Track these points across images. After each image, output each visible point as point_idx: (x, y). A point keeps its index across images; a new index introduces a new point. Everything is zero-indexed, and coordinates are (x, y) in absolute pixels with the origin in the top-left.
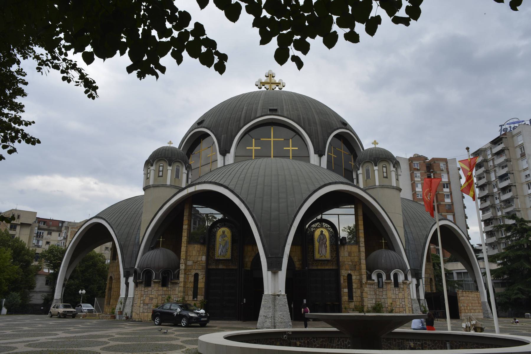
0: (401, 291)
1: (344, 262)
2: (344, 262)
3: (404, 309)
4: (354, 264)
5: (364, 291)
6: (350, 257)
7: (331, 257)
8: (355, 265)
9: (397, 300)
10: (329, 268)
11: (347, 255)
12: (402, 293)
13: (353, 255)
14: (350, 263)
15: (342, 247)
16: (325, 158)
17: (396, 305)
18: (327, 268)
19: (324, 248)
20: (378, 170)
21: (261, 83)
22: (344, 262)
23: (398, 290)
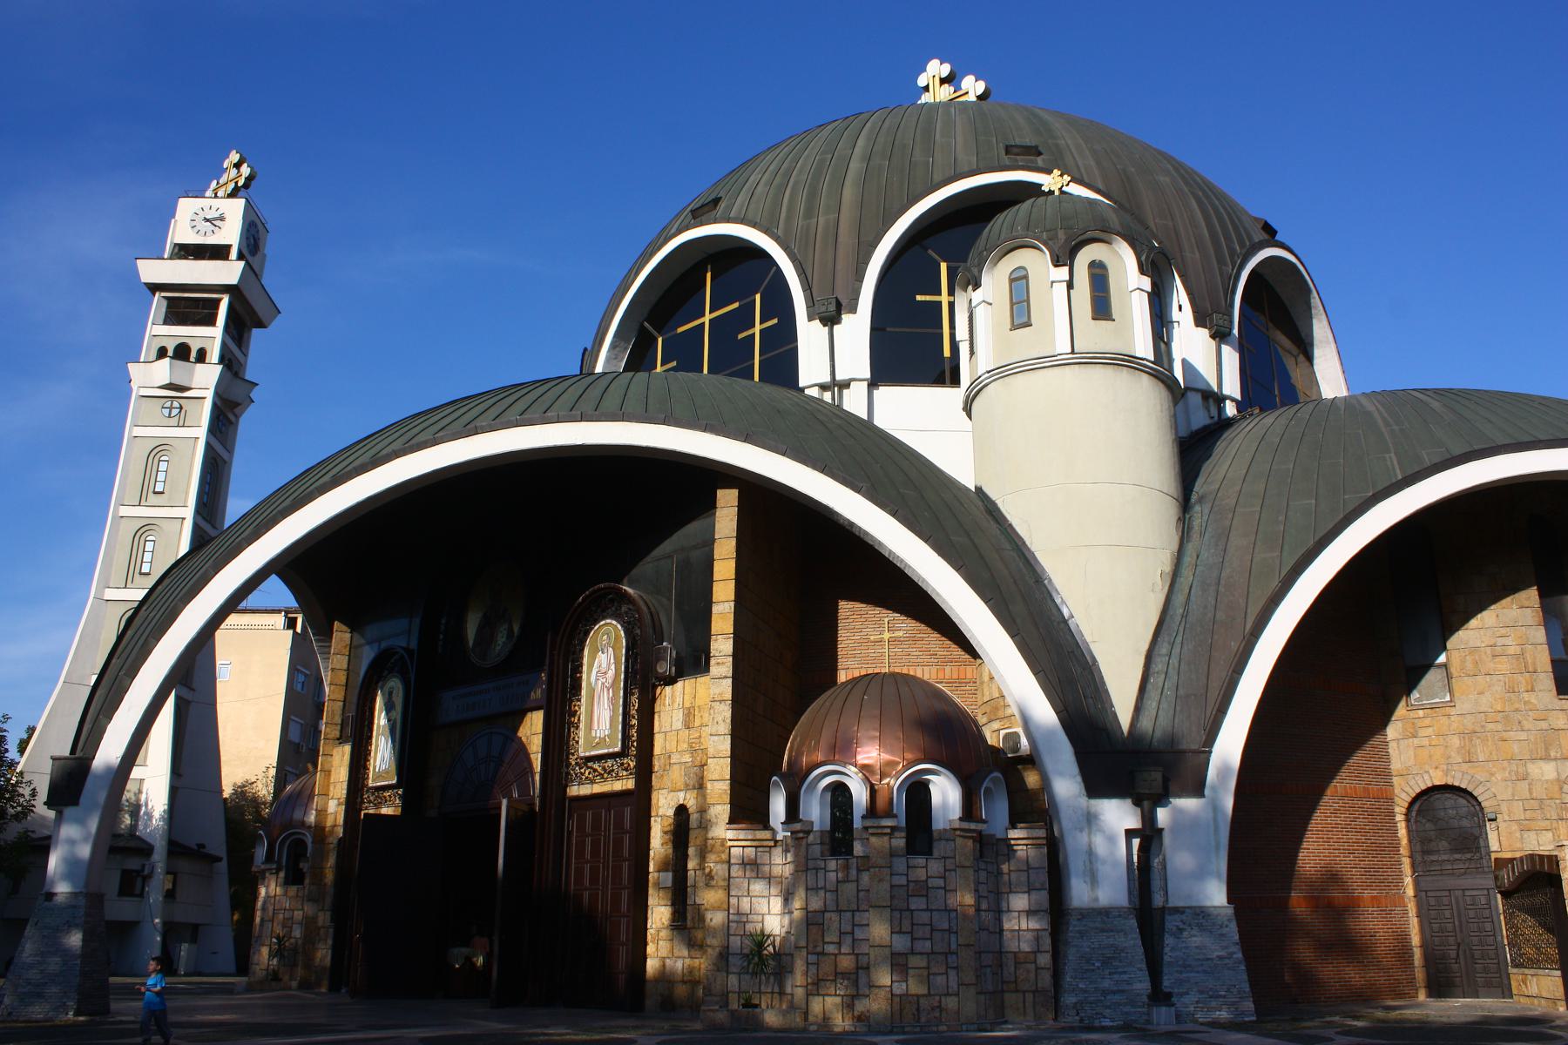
0: (853, 872)
1: (670, 756)
3: (864, 960)
4: (698, 763)
5: (713, 879)
6: (687, 731)
7: (626, 737)
8: (703, 766)
9: (831, 919)
10: (624, 788)
11: (678, 724)
12: (857, 881)
13: (696, 725)
14: (687, 758)
15: (668, 689)
16: (856, 329)
17: (824, 943)
18: (618, 786)
19: (606, 705)
23: (836, 871)
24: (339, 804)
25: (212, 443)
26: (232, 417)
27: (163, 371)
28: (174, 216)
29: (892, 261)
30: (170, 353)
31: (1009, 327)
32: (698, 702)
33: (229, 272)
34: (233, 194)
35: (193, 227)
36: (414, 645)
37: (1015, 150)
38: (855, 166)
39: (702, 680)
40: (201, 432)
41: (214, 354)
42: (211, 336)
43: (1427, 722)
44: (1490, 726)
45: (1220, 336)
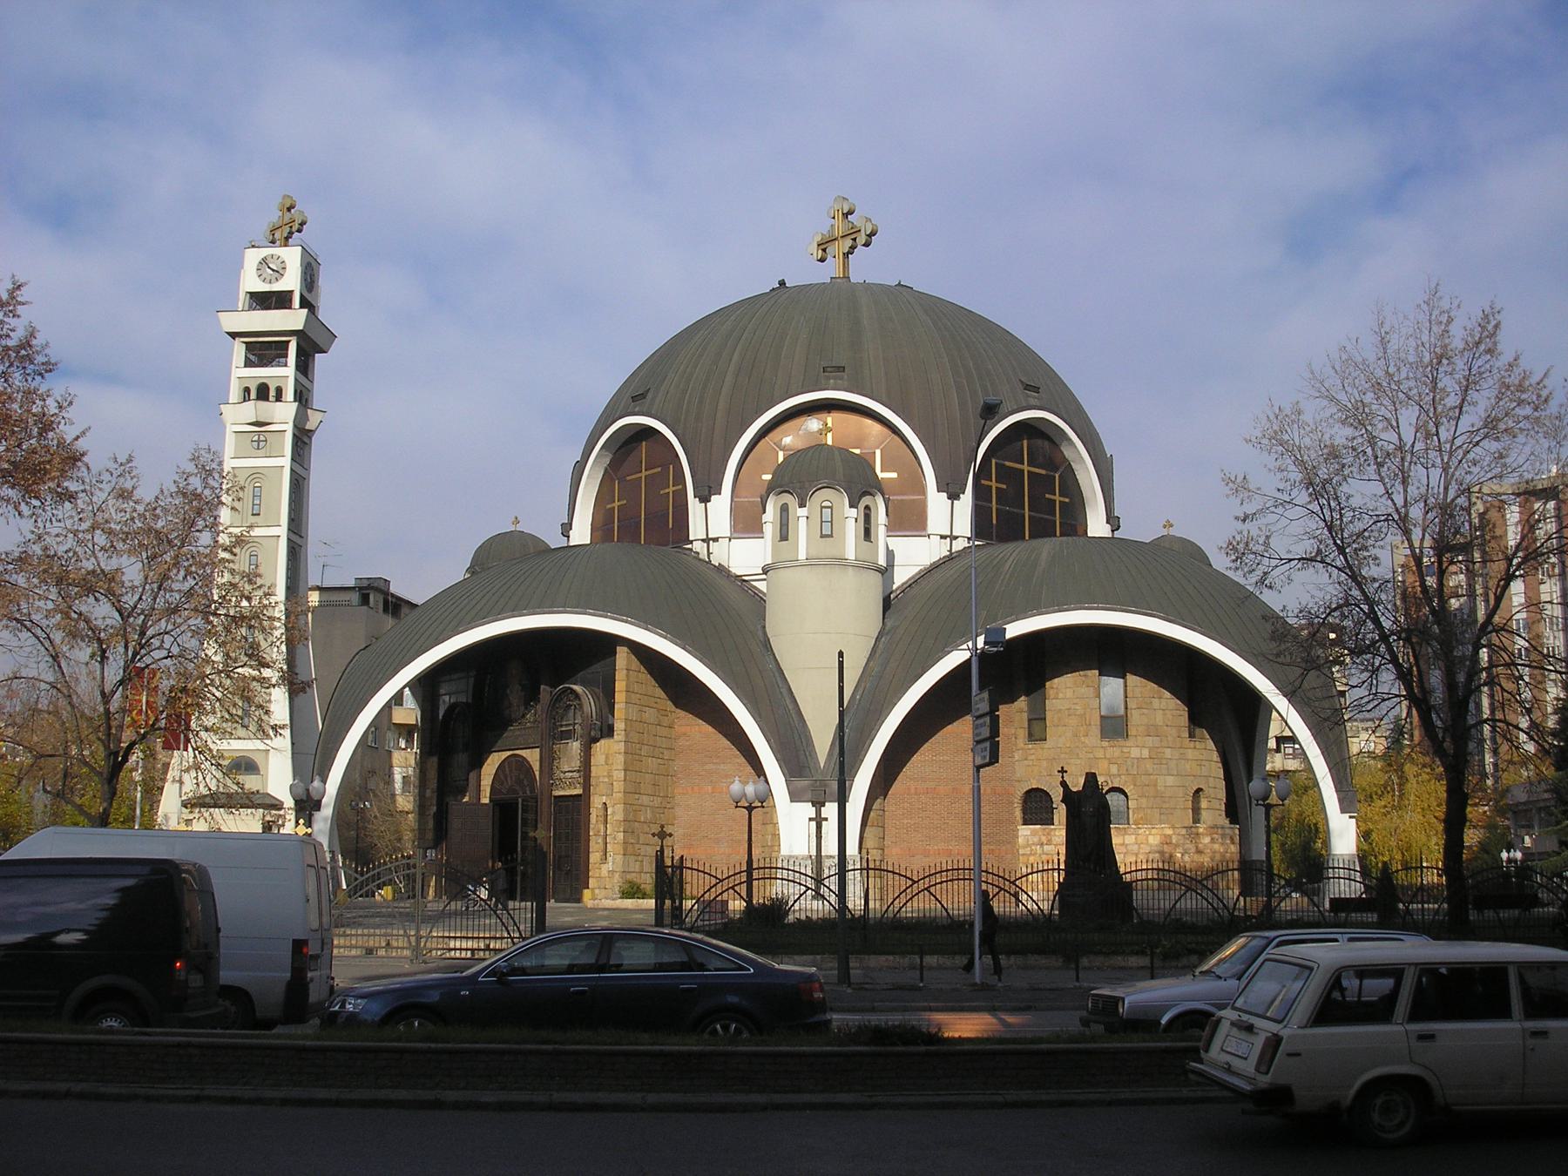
2: (599, 777)
14: (606, 780)
20: (807, 518)
21: (819, 245)
22: (599, 777)
24: (433, 792)
25: (294, 469)
26: (306, 440)
27: (251, 410)
28: (243, 268)
29: (755, 440)
30: (253, 395)
31: (779, 539)
32: (610, 752)
33: (295, 319)
34: (286, 242)
35: (259, 276)
36: (470, 701)
37: (829, 369)
38: (729, 379)
39: (612, 740)
40: (286, 461)
41: (289, 394)
42: (284, 374)
43: (1032, 751)
44: (1063, 756)
45: (954, 497)
